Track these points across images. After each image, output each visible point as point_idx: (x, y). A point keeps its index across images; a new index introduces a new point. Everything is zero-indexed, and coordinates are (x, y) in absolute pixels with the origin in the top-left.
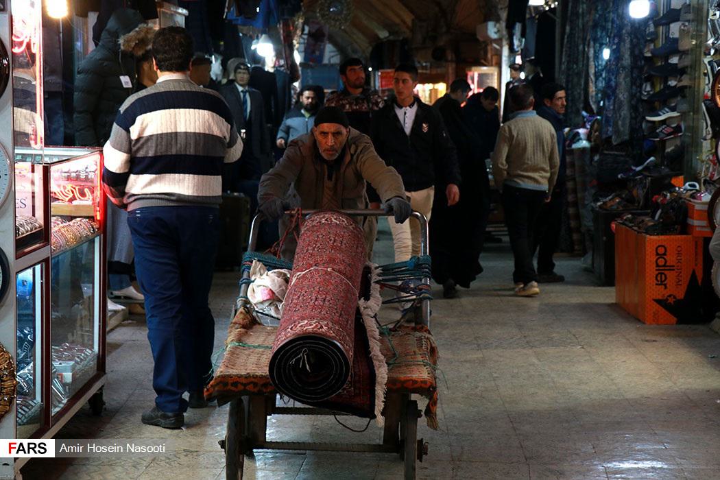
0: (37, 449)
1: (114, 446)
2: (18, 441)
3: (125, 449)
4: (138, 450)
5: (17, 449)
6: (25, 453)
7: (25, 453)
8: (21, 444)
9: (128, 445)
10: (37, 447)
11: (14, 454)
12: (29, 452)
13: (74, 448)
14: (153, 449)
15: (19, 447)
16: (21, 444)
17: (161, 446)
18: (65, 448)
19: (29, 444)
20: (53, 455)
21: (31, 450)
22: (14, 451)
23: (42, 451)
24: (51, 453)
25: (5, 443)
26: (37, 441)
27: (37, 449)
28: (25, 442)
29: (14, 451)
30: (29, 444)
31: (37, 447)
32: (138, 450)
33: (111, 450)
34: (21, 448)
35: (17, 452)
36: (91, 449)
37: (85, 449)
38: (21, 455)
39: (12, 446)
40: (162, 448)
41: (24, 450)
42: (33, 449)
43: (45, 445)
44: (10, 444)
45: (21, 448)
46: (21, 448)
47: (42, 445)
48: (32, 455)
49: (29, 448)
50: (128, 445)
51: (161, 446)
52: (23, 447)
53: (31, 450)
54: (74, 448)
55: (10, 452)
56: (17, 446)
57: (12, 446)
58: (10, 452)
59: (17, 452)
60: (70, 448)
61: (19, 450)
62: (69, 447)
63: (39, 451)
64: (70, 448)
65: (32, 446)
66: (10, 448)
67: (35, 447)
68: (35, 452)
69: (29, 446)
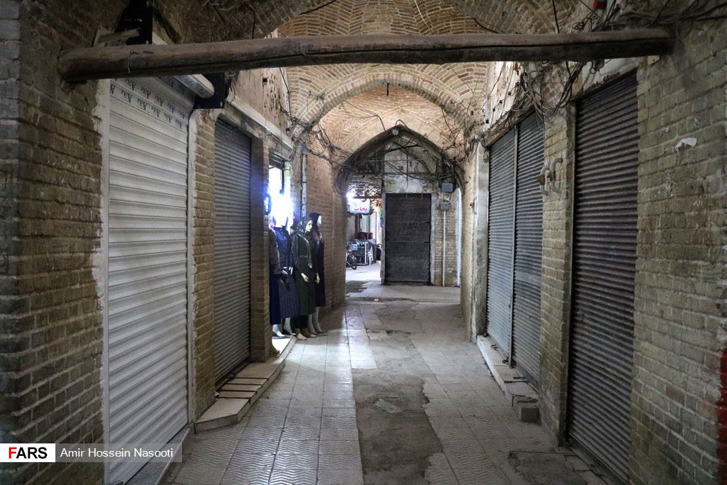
0: (38, 454)
1: (121, 451)
2: (18, 446)
3: (132, 453)
4: (145, 455)
5: (17, 454)
6: (25, 457)
7: (25, 457)
8: (21, 449)
9: (135, 449)
10: (38, 451)
11: (14, 459)
12: (29, 457)
13: (75, 453)
14: (161, 454)
15: (20, 452)
16: (21, 449)
17: (168, 451)
18: (66, 453)
19: (29, 449)
20: (53, 460)
21: (31, 455)
22: (14, 456)
23: (43, 455)
24: (51, 458)
25: (5, 447)
26: (38, 446)
27: (38, 454)
28: (25, 446)
29: (14, 456)
30: (29, 449)
31: (38, 451)
32: (145, 455)
33: (118, 455)
34: (21, 453)
35: (18, 457)
36: (92, 454)
37: (86, 454)
38: (21, 460)
39: (12, 450)
40: (170, 455)
41: (24, 455)
42: (33, 453)
43: (45, 449)
44: (10, 449)
45: (21, 453)
46: (21, 453)
47: (42, 450)
48: (32, 460)
49: (29, 453)
50: (135, 449)
51: (168, 451)
52: (23, 452)
53: (31, 455)
54: (75, 453)
55: (10, 457)
56: (17, 451)
57: (12, 450)
58: (10, 457)
59: (18, 457)
60: (71, 453)
61: (19, 455)
62: (69, 452)
63: (39, 456)
64: (71, 453)
65: (32, 451)
66: (10, 453)
67: (36, 452)
68: (36, 457)
69: (29, 451)
